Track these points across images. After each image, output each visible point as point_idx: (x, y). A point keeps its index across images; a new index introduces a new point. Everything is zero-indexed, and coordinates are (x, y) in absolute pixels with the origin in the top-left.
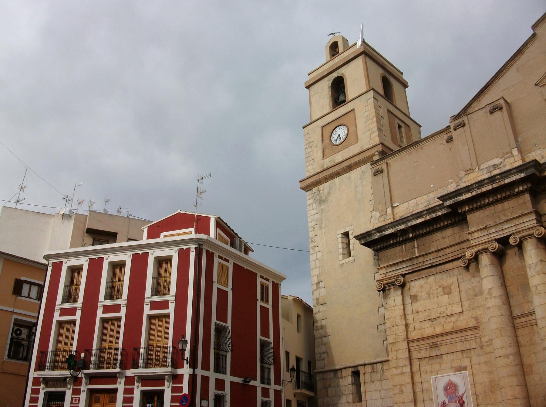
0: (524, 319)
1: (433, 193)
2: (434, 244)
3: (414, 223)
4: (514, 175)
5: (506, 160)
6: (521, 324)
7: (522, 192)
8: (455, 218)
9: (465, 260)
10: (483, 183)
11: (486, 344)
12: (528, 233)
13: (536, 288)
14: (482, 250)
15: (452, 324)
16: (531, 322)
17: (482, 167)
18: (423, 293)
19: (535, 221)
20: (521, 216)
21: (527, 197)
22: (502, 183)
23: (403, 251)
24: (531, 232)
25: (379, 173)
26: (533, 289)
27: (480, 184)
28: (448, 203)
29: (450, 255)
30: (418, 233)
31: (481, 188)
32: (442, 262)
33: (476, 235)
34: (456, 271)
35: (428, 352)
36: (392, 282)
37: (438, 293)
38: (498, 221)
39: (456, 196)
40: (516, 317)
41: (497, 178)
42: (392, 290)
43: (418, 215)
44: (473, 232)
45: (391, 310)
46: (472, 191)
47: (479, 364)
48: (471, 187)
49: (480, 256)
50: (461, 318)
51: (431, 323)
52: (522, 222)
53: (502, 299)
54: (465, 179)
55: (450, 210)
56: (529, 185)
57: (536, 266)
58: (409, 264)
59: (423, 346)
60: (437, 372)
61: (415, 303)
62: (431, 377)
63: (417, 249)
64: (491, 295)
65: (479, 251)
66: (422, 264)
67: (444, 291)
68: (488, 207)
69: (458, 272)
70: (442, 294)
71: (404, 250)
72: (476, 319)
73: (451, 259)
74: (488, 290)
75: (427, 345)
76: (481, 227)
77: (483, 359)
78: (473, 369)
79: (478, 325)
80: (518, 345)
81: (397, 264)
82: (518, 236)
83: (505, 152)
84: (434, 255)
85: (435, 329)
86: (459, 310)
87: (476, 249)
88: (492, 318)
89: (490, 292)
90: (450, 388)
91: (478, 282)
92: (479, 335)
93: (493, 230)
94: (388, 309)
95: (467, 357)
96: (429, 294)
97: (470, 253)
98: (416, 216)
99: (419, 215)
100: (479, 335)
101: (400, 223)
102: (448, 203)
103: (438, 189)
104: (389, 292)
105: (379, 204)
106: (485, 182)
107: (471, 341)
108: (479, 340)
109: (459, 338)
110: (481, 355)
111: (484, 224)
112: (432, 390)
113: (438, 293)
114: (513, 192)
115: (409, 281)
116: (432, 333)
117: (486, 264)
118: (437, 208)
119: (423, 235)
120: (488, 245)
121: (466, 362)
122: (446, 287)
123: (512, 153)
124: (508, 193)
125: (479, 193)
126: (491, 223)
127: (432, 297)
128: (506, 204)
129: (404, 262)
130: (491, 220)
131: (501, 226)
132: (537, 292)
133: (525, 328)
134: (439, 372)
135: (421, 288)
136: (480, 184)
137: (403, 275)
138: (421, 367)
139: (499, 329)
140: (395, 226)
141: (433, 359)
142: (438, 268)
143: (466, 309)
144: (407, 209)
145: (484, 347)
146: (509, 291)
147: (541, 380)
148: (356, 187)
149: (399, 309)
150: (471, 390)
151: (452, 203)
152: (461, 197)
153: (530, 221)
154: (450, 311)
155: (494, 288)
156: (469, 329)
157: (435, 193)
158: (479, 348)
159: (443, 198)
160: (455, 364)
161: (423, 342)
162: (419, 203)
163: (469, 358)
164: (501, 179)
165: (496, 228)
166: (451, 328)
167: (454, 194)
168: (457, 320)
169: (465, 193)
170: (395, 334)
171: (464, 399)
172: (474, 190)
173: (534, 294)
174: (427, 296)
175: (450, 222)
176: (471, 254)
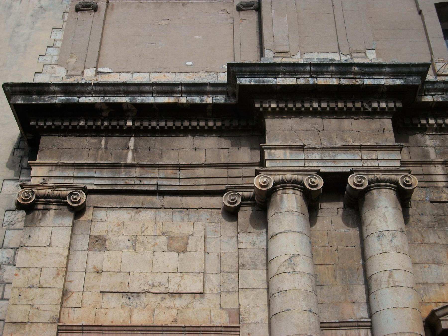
1: (188, 75)
2: (172, 153)
3: (150, 100)
4: (383, 77)
7: (381, 113)
9: (237, 197)
10: (324, 70)
12: (387, 177)
13: (390, 276)
14: (289, 182)
15: (174, 312)
18: (121, 238)
20: (374, 148)
21: (387, 123)
22: (359, 82)
23: (99, 148)
24: (393, 177)
25: (89, 10)
28: (246, 81)
29: (202, 181)
31: (317, 78)
32: (181, 189)
33: (279, 154)
34: (205, 214)
36: (59, 197)
38: (326, 144)
39: (266, 74)
41: (353, 70)
42: (52, 212)
43: (165, 88)
45: (37, 252)
46: (299, 76)
48: (301, 69)
49: (280, 192)
50: (198, 304)
51: (124, 300)
52: (374, 157)
53: (312, 281)
55: (233, 101)
56: (399, 105)
57: (394, 236)
58: (107, 173)
61: (96, 252)
63: (133, 154)
64: (294, 267)
66: (137, 182)
67: (171, 244)
68: (310, 117)
69: (209, 217)
70: (166, 248)
71: (103, 146)
73: (202, 188)
74: (287, 257)
79: (238, 325)
81: (80, 166)
83: (354, 49)
84: (169, 172)
86: (198, 288)
87: (278, 177)
88: (290, 311)
89: (292, 262)
91: (253, 243)
93: (316, 155)
94: (28, 248)
96: (135, 242)
97: (265, 180)
98: (159, 88)
101: (120, 91)
102: (244, 81)
103: (199, 72)
104: (44, 214)
105: (71, 57)
106: (330, 69)
113: (156, 244)
114: (367, 107)
115: (94, 207)
116: (124, 321)
117: (290, 209)
119: (153, 132)
120: (304, 177)
122: (177, 237)
123: (366, 54)
127: (142, 249)
129: (96, 166)
130: (313, 139)
131: (334, 154)
136: (319, 69)
137: (89, 192)
140: (106, 93)
142: (167, 200)
148: (19, 25)
149: (57, 254)
152: (275, 80)
155: (302, 257)
156: (214, 329)
157: (191, 76)
164: (359, 75)
165: (321, 154)
166: (171, 319)
168: (187, 307)
169: (285, 75)
170: (32, 305)
172: (303, 76)
173: (384, 285)
174: (129, 244)
175: (219, 124)
176: (264, 183)
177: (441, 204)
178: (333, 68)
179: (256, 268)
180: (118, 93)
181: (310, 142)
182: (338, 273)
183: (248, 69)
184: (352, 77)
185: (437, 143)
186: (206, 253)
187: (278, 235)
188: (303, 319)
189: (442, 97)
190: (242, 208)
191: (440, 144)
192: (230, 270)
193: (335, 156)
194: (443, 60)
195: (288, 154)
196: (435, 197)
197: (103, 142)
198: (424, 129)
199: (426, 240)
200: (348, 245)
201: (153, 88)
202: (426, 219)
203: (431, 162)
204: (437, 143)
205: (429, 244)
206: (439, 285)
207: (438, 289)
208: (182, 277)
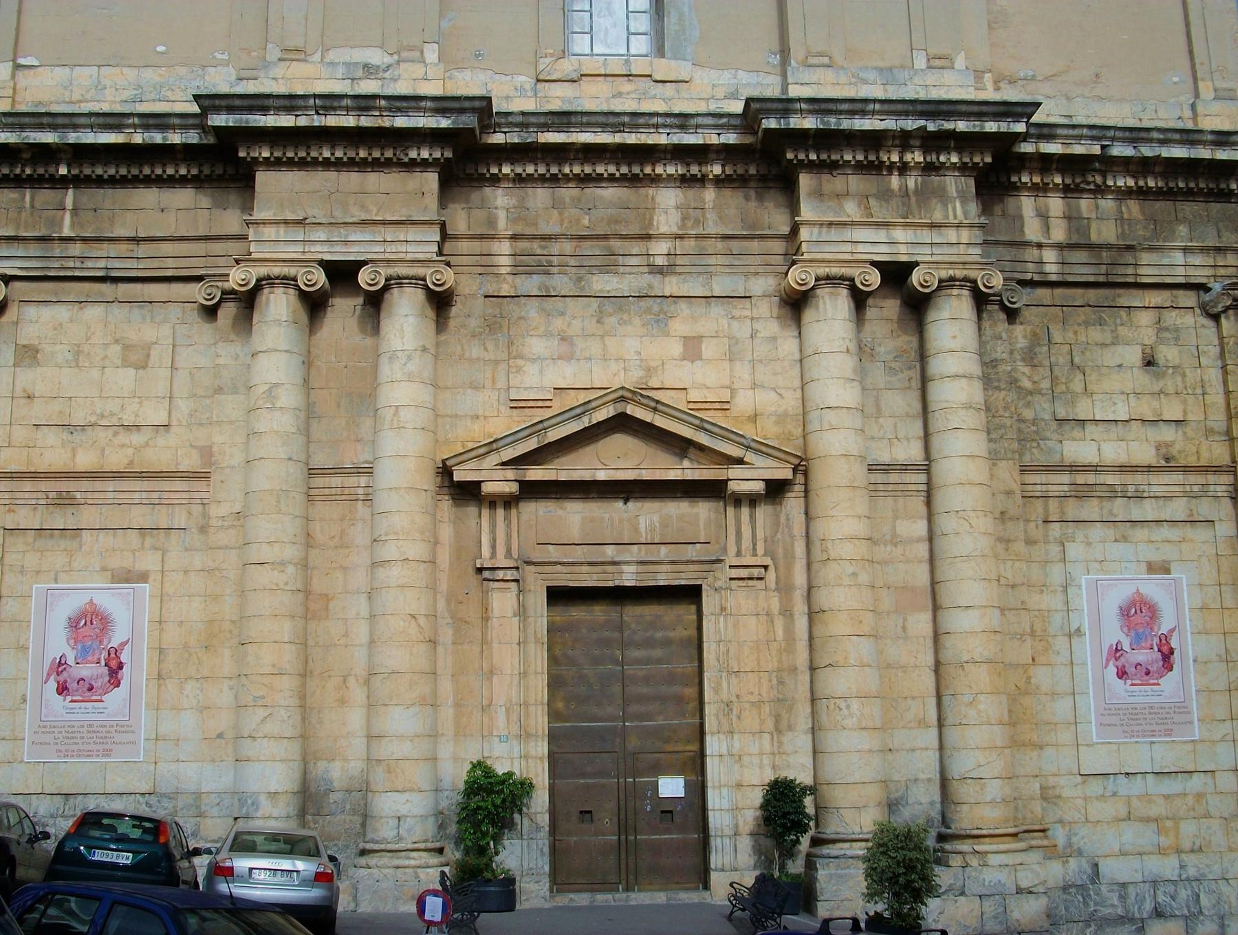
0: (336, 481)
1: (159, 71)
3: (88, 137)
5: (403, 65)
6: (327, 491)
7: (424, 164)
8: (213, 165)
9: (214, 290)
10: (336, 104)
11: (220, 523)
13: (396, 413)
15: (130, 451)
16: (353, 491)
17: (332, 56)
18: (58, 347)
19: (436, 249)
21: (431, 179)
22: (386, 123)
23: (21, 209)
24: (419, 271)
26: (388, 414)
27: (329, 102)
29: (170, 263)
30: (87, 171)
32: (140, 274)
33: (269, 232)
34: (175, 311)
35: (39, 514)
37: (106, 357)
38: (339, 216)
39: (251, 109)
43: (110, 120)
47: (186, 572)
48: (301, 103)
49: (266, 291)
50: (161, 441)
51: (66, 436)
53: (298, 417)
54: (279, 70)
56: (448, 154)
57: (409, 358)
58: (34, 250)
59: (27, 495)
60: (56, 575)
62: (35, 586)
63: (72, 217)
65: (269, 278)
66: (78, 265)
70: (119, 363)
71: (28, 205)
72: (207, 453)
73: (169, 273)
74: (266, 387)
75: (40, 495)
76: (291, 217)
77: (198, 561)
78: (165, 580)
80: (308, 540)
82: (385, 272)
83: (405, 43)
84: (123, 248)
85: (74, 456)
86: (161, 418)
87: (263, 271)
90: (88, 623)
92: (204, 495)
93: (321, 235)
95: (156, 549)
96: (78, 353)
98: (101, 120)
99: (113, 121)
100: (204, 495)
101: (42, 124)
102: (219, 120)
103: (177, 65)
106: (344, 102)
107: (177, 508)
108: (200, 508)
109: (144, 495)
110: (196, 550)
111: (299, 212)
112: (29, 622)
114: (402, 156)
116: (65, 464)
117: (278, 317)
118: (177, 121)
119: (100, 182)
121: (149, 562)
122: (134, 346)
123: (422, 52)
124: (389, 154)
125: (316, 124)
126: (317, 212)
127: (87, 365)
128: (374, 180)
132: (395, 422)
134: (61, 575)
135: (55, 329)
136: (328, 103)
138: (6, 554)
140: (22, 127)
141: (52, 536)
143: (179, 421)
144: (65, 88)
145: (212, 530)
146: (315, 403)
147: (346, 635)
150: (149, 635)
151: (231, 124)
153: (423, 243)
154: (133, 416)
155: (286, 386)
156: (179, 475)
158: (194, 530)
159: (209, 102)
160: (115, 563)
161: (28, 486)
162: (107, 82)
163: (161, 552)
166: (126, 461)
167: (246, 103)
168: (147, 445)
171: (124, 657)
174: (70, 356)
175: (194, 171)
177: (500, 299)
178: (350, 102)
179: (237, 393)
180: (40, 127)
181: (315, 212)
183: (224, 103)
184: (378, 114)
185: (513, 202)
186: (173, 368)
187: (260, 354)
189: (519, 136)
190: (223, 304)
191: (516, 203)
193: (346, 236)
194: (552, 51)
195: (283, 233)
197: (28, 198)
198: (495, 180)
199: (467, 355)
202: (473, 323)
204: (513, 202)
205: (470, 360)
206: (472, 417)
207: (469, 422)
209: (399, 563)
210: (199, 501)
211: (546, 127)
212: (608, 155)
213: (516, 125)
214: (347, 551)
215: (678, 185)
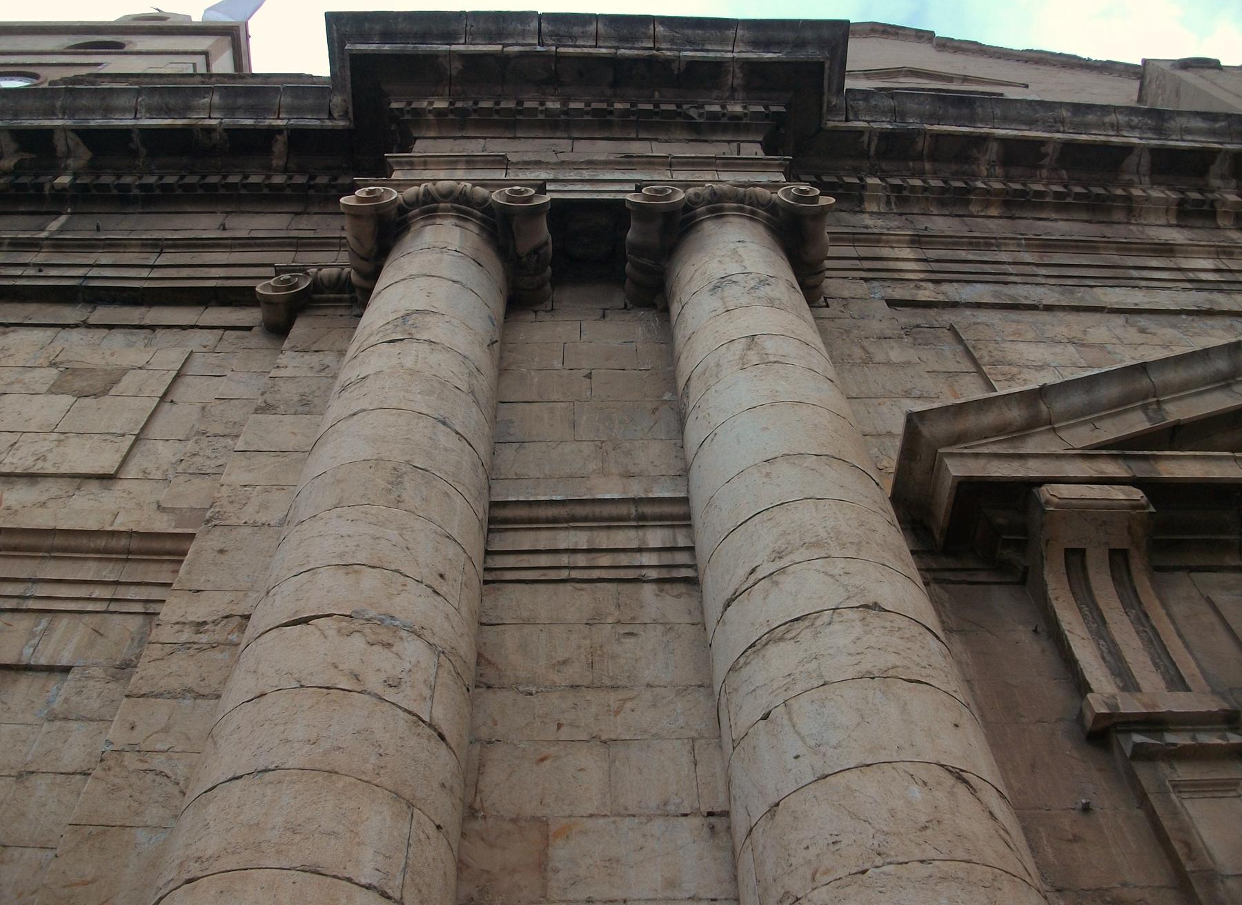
6: (543, 560)
20: (709, 164)
40: (523, 512)
44: (425, 163)
79: (190, 531)
92: (156, 593)
98: (156, 100)
100: (156, 593)
114: (693, 112)
133: (569, 587)
139: (390, 466)
158: (98, 672)
182: (585, 418)
188: (406, 428)
192: (226, 431)
196: (899, 293)
200: (628, 367)
201: (140, 99)
203: (877, 237)
208: (60, 441)
209: (850, 614)
210: (138, 608)
211: (934, 118)
212: (1045, 173)
213: (884, 113)
214: (613, 698)
215: (1174, 222)
